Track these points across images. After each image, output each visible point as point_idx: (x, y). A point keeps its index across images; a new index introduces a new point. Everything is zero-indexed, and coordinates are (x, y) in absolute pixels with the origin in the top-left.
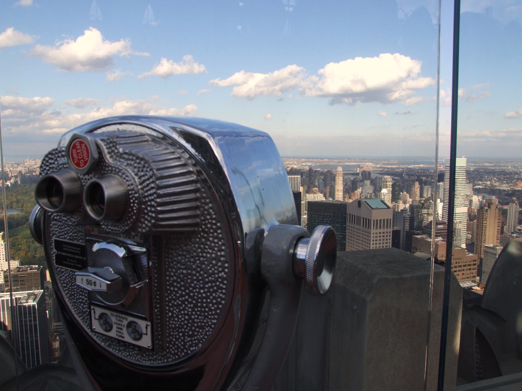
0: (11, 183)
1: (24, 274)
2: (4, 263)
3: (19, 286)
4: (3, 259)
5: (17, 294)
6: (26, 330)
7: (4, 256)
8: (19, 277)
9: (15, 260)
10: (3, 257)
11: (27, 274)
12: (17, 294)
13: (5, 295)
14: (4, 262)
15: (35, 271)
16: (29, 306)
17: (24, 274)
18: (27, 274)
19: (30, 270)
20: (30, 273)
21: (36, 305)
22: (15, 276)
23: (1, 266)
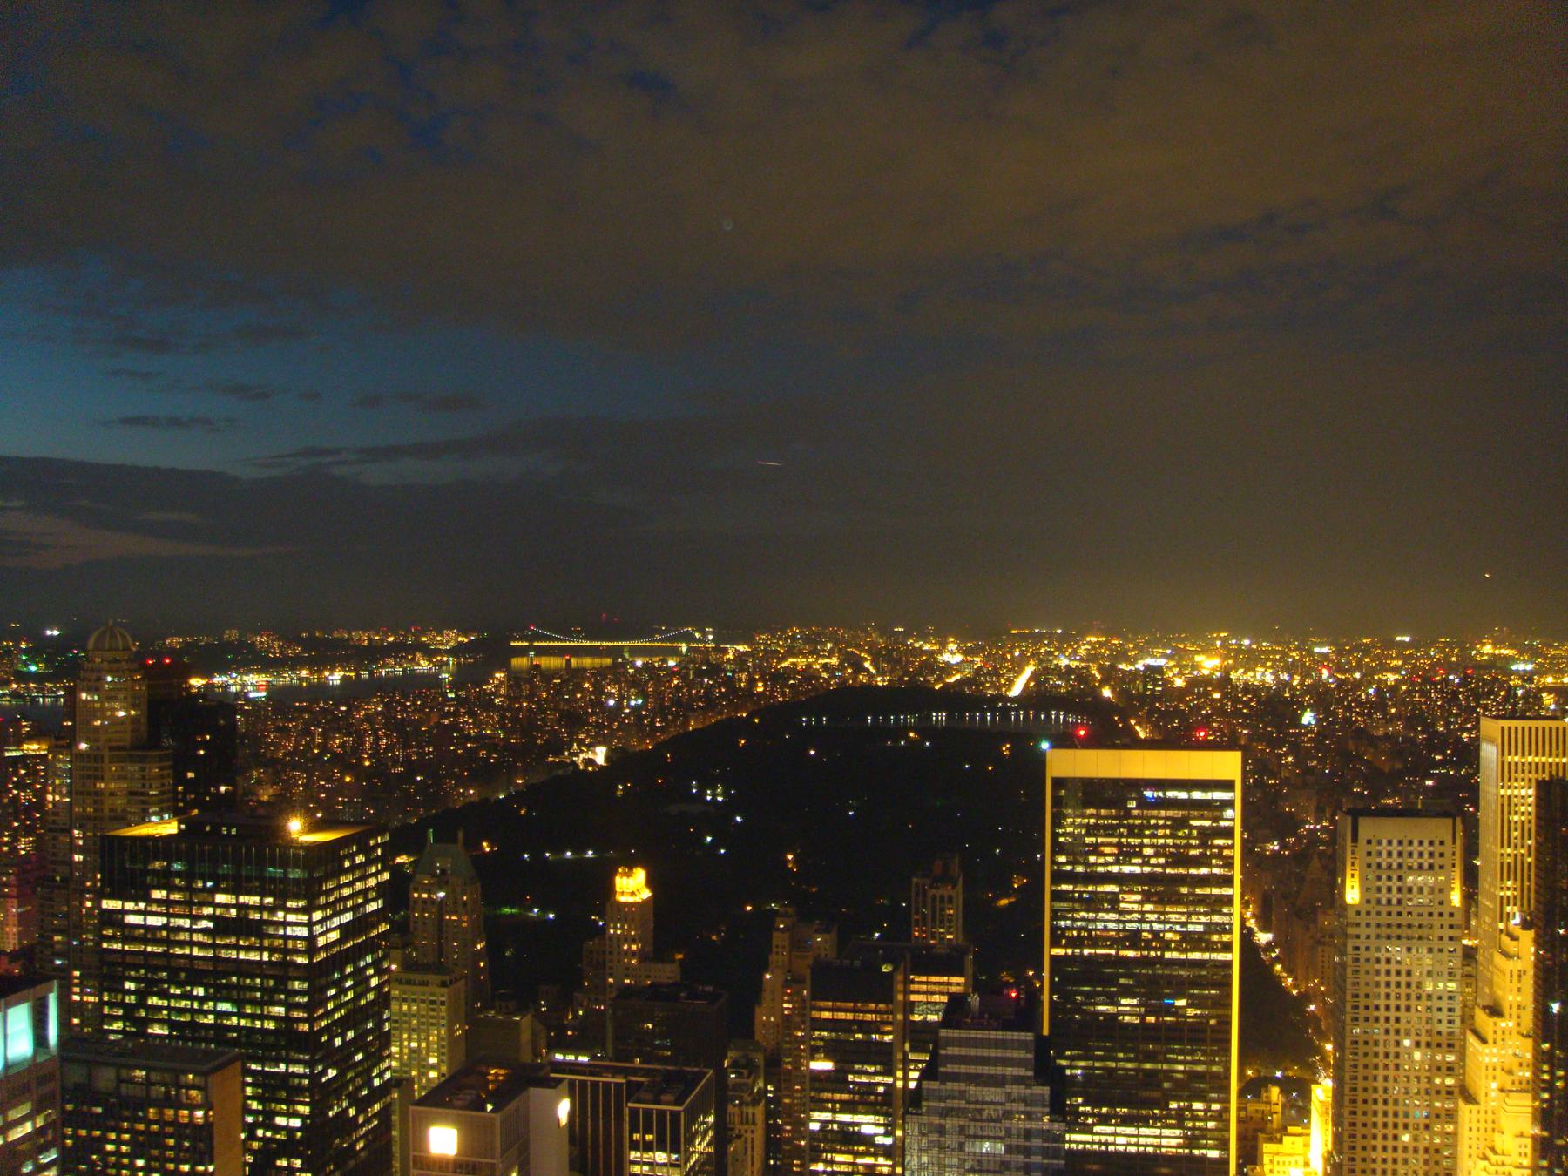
16: (661, 1114)
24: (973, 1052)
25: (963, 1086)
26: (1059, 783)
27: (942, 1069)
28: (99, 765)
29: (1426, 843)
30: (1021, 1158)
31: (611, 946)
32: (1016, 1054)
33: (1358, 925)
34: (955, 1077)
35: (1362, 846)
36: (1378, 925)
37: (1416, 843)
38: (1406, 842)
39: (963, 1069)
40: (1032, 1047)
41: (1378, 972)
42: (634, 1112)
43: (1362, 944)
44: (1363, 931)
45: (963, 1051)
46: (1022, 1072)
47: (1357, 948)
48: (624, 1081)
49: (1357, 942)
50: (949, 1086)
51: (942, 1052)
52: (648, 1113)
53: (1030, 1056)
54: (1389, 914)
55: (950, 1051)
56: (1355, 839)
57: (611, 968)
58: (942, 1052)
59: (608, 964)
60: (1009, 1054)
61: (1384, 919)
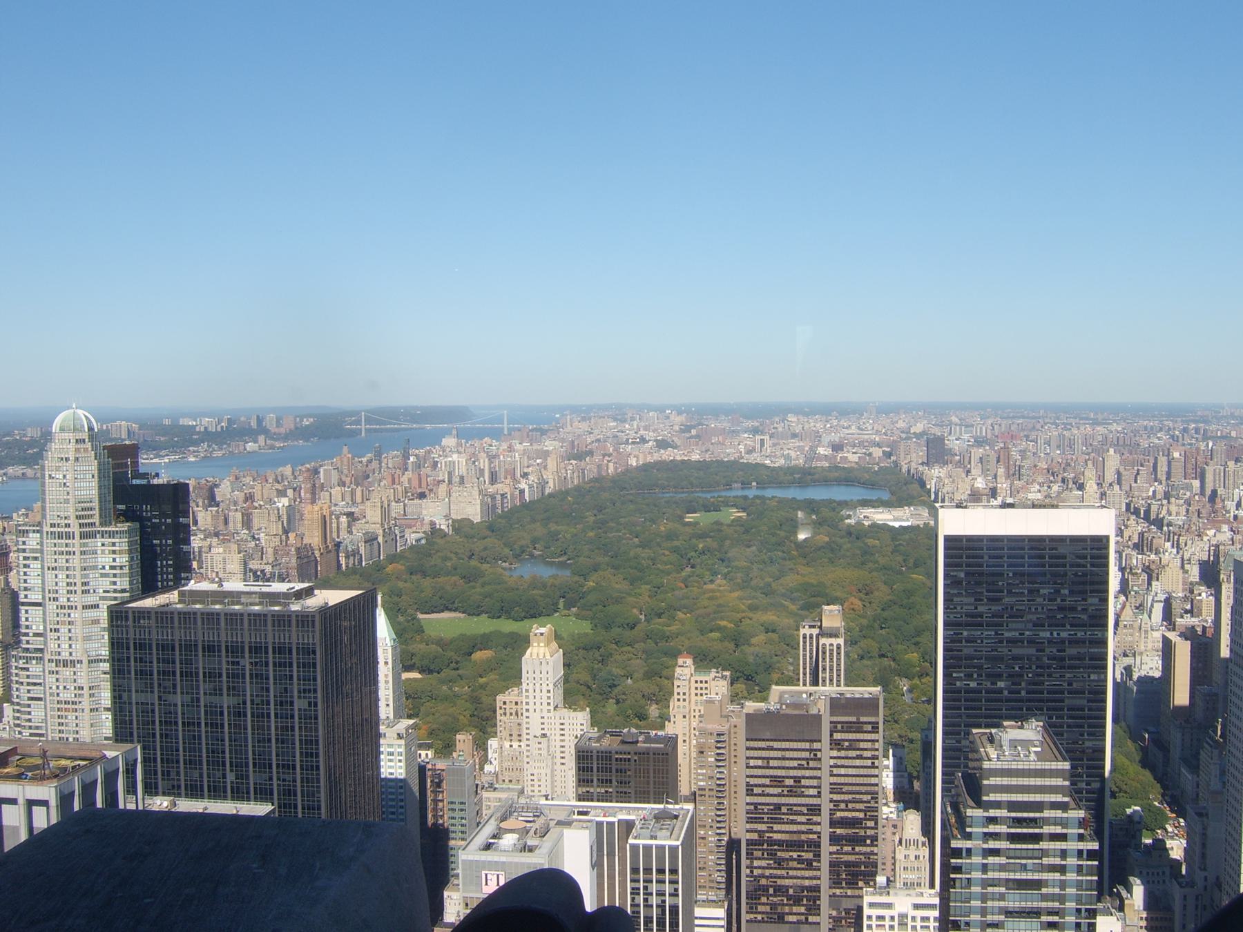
0: (531, 487)
3: (611, 787)
4: (549, 704)
5: (621, 809)
7: (551, 695)
8: (614, 761)
9: (575, 710)
10: (549, 698)
11: (635, 753)
12: (621, 809)
13: (591, 807)
15: (657, 748)
16: (661, 848)
17: (629, 753)
18: (635, 753)
19: (644, 742)
20: (644, 750)
21: (680, 847)
23: (543, 724)
24: (1014, 781)
25: (1002, 813)
26: (948, 539)
27: (985, 798)
28: (70, 541)
30: (1057, 876)
31: (527, 697)
34: (997, 805)
39: (1004, 797)
40: (1067, 775)
42: (635, 848)
45: (1005, 781)
46: (1059, 798)
48: (615, 820)
50: (993, 813)
51: (985, 782)
52: (648, 848)
53: (1067, 783)
55: (993, 781)
57: (527, 717)
58: (985, 782)
59: (525, 714)
60: (1048, 782)
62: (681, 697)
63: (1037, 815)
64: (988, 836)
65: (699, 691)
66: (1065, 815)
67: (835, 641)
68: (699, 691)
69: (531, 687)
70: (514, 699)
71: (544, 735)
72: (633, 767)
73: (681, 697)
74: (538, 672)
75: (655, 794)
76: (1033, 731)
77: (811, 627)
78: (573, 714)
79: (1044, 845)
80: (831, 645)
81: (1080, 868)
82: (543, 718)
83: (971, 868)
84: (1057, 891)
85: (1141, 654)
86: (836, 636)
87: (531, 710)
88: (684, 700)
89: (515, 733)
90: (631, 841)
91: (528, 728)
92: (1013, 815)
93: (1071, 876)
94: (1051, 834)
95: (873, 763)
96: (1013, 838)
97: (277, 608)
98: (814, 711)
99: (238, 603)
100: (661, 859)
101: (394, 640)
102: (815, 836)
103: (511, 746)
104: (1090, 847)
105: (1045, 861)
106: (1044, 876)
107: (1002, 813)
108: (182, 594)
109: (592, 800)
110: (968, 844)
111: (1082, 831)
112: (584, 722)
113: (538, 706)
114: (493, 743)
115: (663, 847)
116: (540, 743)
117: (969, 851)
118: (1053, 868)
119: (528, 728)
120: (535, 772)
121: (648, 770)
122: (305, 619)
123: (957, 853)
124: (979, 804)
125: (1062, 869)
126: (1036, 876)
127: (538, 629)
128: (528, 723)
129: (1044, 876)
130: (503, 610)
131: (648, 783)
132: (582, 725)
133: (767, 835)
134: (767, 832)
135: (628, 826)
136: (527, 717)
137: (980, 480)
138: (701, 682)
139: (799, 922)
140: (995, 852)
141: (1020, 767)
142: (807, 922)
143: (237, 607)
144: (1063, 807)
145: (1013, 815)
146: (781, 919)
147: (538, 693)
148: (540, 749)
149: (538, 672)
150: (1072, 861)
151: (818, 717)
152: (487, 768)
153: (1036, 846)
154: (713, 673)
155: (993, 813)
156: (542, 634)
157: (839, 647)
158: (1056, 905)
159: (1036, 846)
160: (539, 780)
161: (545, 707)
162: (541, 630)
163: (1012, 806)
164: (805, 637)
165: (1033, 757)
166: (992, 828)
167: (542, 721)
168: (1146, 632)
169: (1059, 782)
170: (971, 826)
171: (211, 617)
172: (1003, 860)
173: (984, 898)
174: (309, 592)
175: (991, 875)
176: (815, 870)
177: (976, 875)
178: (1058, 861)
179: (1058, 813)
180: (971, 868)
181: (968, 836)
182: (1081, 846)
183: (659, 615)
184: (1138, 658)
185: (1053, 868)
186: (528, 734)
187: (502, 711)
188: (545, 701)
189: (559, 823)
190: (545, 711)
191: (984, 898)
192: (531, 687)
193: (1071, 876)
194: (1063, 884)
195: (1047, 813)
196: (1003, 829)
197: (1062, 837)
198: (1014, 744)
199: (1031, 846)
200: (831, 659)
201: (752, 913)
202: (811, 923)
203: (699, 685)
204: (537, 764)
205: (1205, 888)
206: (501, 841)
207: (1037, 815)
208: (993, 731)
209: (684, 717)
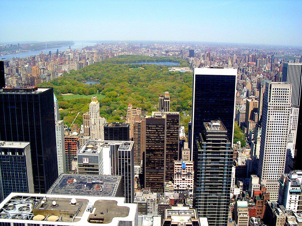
1: (117, 128)
2: (96, 119)
6: (123, 169)
14: (96, 118)
18: (119, 128)
22: (111, 129)
24: (214, 135)
25: (211, 143)
26: (196, 75)
27: (207, 139)
29: (285, 89)
30: (223, 158)
31: (91, 114)
32: (223, 135)
33: (270, 107)
34: (210, 141)
35: (272, 90)
36: (274, 107)
37: (283, 89)
38: (281, 89)
39: (211, 139)
41: (273, 117)
43: (271, 111)
44: (271, 108)
45: (212, 135)
46: (224, 139)
47: (269, 112)
48: (115, 145)
49: (269, 111)
50: (208, 143)
51: (207, 135)
52: (123, 152)
54: (276, 104)
55: (209, 135)
56: (270, 88)
57: (91, 119)
58: (207, 135)
59: (90, 119)
61: (275, 106)
62: (129, 114)
63: (219, 143)
64: (207, 149)
65: (134, 113)
66: (226, 143)
67: (168, 100)
68: (134, 113)
69: (91, 112)
70: (87, 115)
71: (95, 124)
72: (118, 132)
73: (129, 114)
74: (93, 108)
75: (124, 138)
76: (218, 123)
77: (161, 97)
78: (102, 119)
79: (220, 151)
80: (167, 102)
81: (229, 156)
82: (95, 119)
83: (202, 156)
84: (223, 161)
85: (241, 104)
86: (168, 99)
87: (92, 118)
88: (130, 115)
89: (88, 123)
90: (119, 150)
91: (91, 122)
92: (213, 143)
93: (227, 158)
94: (222, 148)
95: (177, 131)
96: (213, 149)
97: (29, 93)
98: (163, 117)
99: (19, 92)
100: (126, 154)
101: (57, 101)
102: (163, 149)
103: (87, 127)
104: (231, 151)
105: (221, 154)
106: (220, 158)
107: (211, 143)
108: (4, 90)
109: (108, 140)
110: (203, 150)
111: (229, 147)
112: (105, 120)
113: (93, 117)
114: (82, 126)
115: (127, 151)
116: (94, 126)
117: (202, 152)
118: (222, 156)
119: (91, 122)
120: (93, 133)
121: (122, 132)
122: (36, 96)
123: (200, 153)
124: (205, 141)
125: (224, 156)
126: (218, 158)
127: (93, 97)
128: (91, 121)
129: (220, 158)
130: (84, 93)
131: (122, 135)
132: (104, 121)
133: (151, 148)
134: (151, 147)
135: (118, 146)
136: (91, 119)
137: (203, 61)
138: (134, 110)
139: (159, 169)
140: (209, 152)
141: (215, 132)
142: (161, 169)
143: (18, 93)
144: (225, 141)
145: (213, 143)
146: (154, 168)
147: (93, 114)
148: (94, 127)
149: (93, 108)
150: (227, 154)
151: (164, 119)
152: (81, 132)
153: (219, 151)
154: (137, 109)
155: (208, 143)
156: (94, 99)
157: (169, 102)
158: (223, 165)
159: (219, 151)
160: (94, 135)
161: (95, 117)
162: (94, 97)
163: (213, 141)
164: (160, 99)
165: (218, 129)
166: (208, 147)
167: (95, 120)
168: (242, 99)
169: (225, 135)
170: (203, 146)
171: (12, 96)
172: (211, 154)
173: (206, 163)
174: (36, 89)
175: (207, 158)
176: (163, 156)
177: (204, 158)
178: (224, 154)
179: (224, 143)
180: (202, 156)
181: (202, 149)
182: (229, 151)
183: (123, 94)
184: (240, 106)
185: (222, 156)
186: (91, 124)
187: (84, 118)
188: (95, 115)
189: (101, 146)
190: (95, 118)
191: (206, 163)
192: (91, 112)
193: (227, 158)
194: (224, 160)
195: (221, 143)
196: (211, 147)
197: (225, 149)
198: (214, 126)
199: (217, 151)
200: (167, 106)
201: (147, 167)
202: (162, 169)
203: (134, 111)
204: (93, 131)
205: (255, 160)
206: (87, 150)
207: (219, 143)
208: (209, 123)
209: (130, 119)
